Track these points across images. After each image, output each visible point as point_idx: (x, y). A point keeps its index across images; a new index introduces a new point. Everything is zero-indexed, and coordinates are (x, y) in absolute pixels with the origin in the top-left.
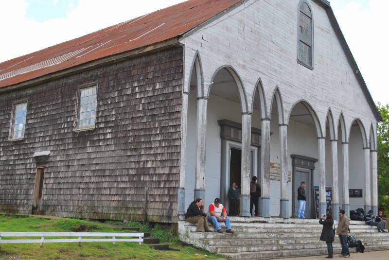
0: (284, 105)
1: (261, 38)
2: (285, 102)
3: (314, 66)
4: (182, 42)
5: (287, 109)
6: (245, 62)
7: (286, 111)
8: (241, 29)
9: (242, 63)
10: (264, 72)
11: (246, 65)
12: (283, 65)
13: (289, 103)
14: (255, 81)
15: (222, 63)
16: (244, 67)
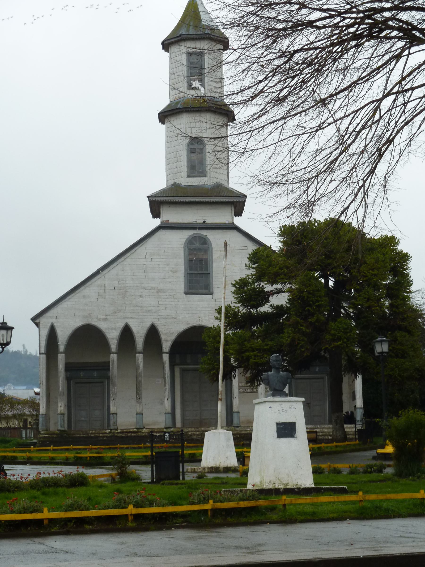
0: (163, 337)
1: (128, 290)
2: (166, 334)
3: (215, 290)
4: (37, 321)
5: (169, 339)
6: (106, 315)
7: (167, 341)
8: (102, 291)
9: (104, 317)
10: (134, 316)
11: (108, 317)
12: (160, 303)
13: (173, 333)
14: (120, 326)
15: (78, 323)
16: (105, 320)
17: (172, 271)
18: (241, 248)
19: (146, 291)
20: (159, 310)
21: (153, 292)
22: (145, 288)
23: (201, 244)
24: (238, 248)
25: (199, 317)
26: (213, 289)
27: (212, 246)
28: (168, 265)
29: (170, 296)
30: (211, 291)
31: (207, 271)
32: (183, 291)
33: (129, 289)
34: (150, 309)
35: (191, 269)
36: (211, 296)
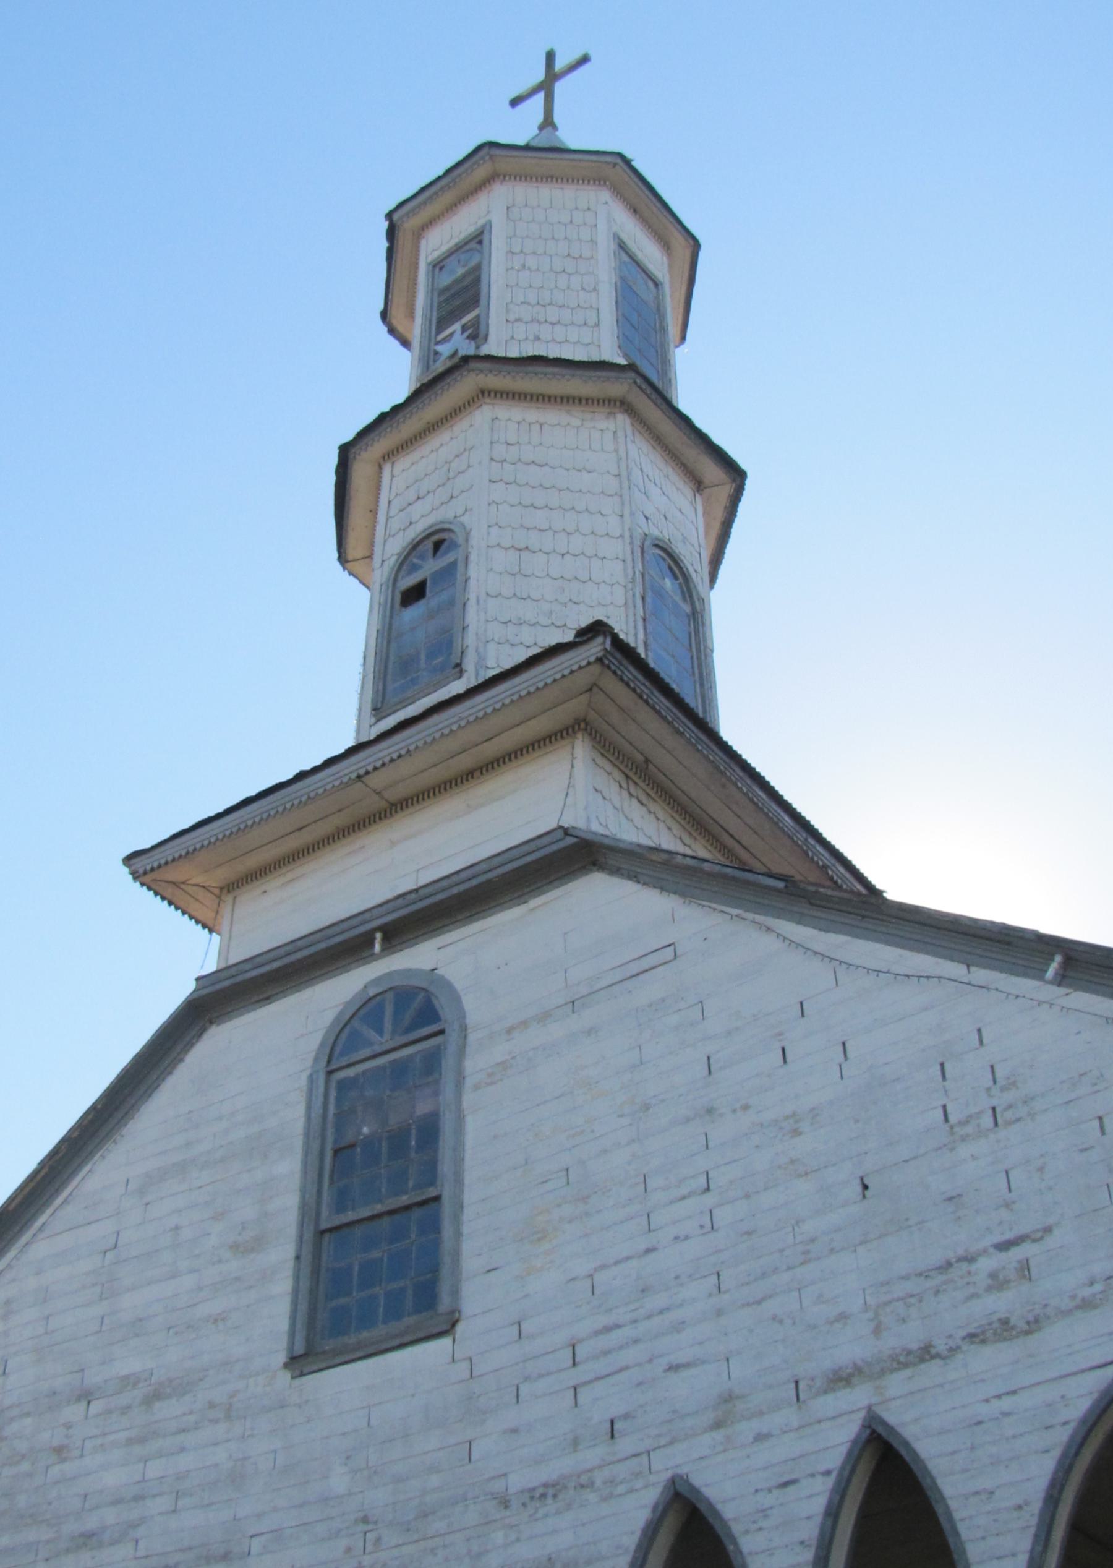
17: (235, 1247)
18: (635, 968)
19: (96, 1407)
20: (142, 1520)
21: (125, 1410)
22: (86, 1396)
23: (409, 1030)
24: (618, 975)
25: (365, 1520)
26: (456, 1293)
27: (462, 1016)
28: (218, 1217)
29: (212, 1405)
30: (445, 1303)
31: (432, 1182)
32: (282, 1357)
33: (12, 1419)
34: (91, 1523)
35: (341, 1202)
36: (445, 1342)
